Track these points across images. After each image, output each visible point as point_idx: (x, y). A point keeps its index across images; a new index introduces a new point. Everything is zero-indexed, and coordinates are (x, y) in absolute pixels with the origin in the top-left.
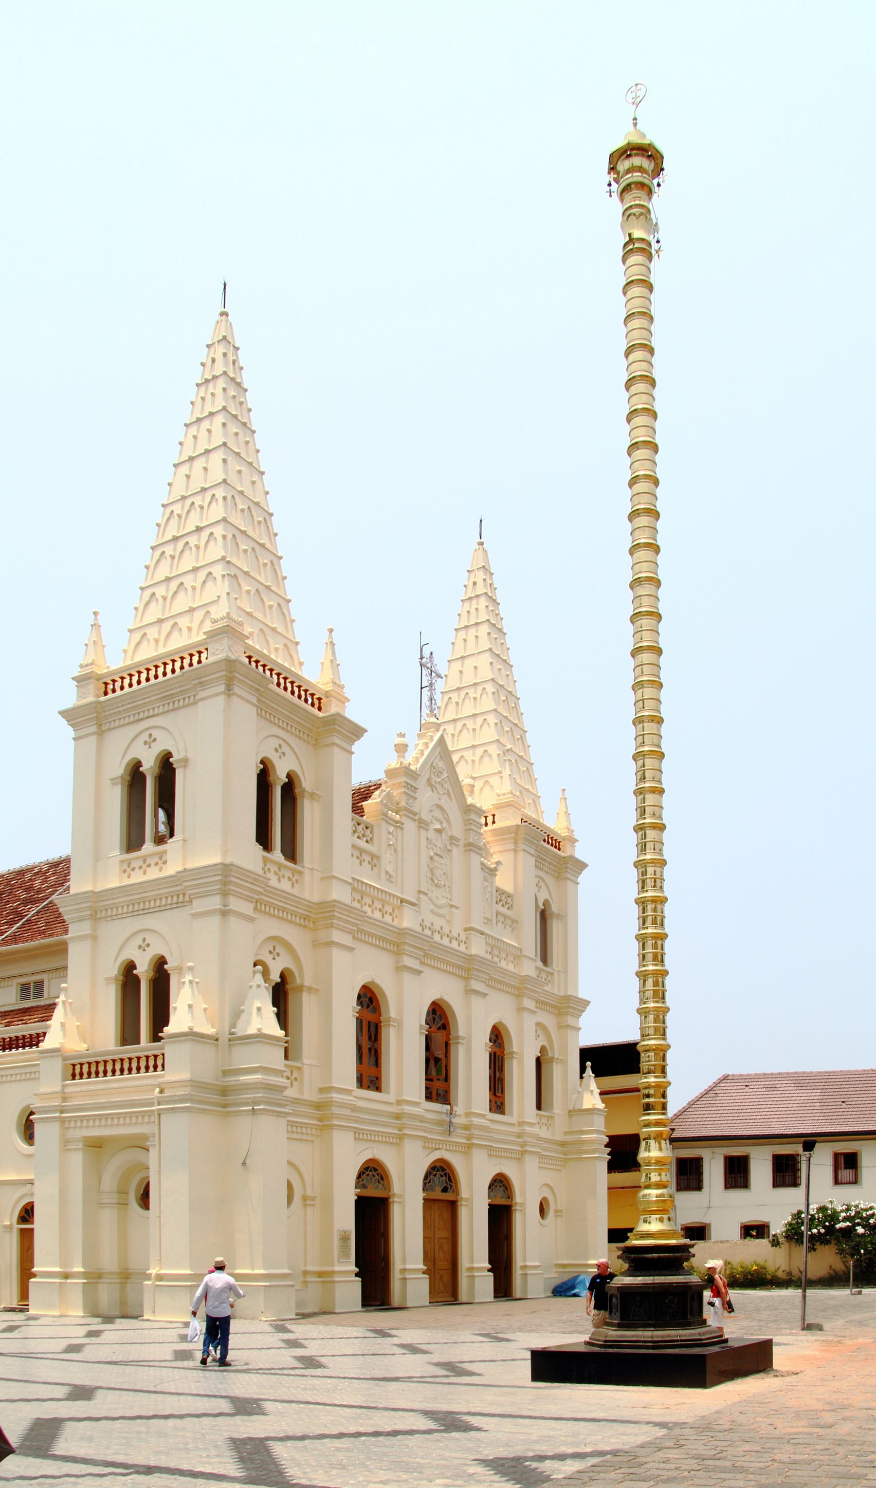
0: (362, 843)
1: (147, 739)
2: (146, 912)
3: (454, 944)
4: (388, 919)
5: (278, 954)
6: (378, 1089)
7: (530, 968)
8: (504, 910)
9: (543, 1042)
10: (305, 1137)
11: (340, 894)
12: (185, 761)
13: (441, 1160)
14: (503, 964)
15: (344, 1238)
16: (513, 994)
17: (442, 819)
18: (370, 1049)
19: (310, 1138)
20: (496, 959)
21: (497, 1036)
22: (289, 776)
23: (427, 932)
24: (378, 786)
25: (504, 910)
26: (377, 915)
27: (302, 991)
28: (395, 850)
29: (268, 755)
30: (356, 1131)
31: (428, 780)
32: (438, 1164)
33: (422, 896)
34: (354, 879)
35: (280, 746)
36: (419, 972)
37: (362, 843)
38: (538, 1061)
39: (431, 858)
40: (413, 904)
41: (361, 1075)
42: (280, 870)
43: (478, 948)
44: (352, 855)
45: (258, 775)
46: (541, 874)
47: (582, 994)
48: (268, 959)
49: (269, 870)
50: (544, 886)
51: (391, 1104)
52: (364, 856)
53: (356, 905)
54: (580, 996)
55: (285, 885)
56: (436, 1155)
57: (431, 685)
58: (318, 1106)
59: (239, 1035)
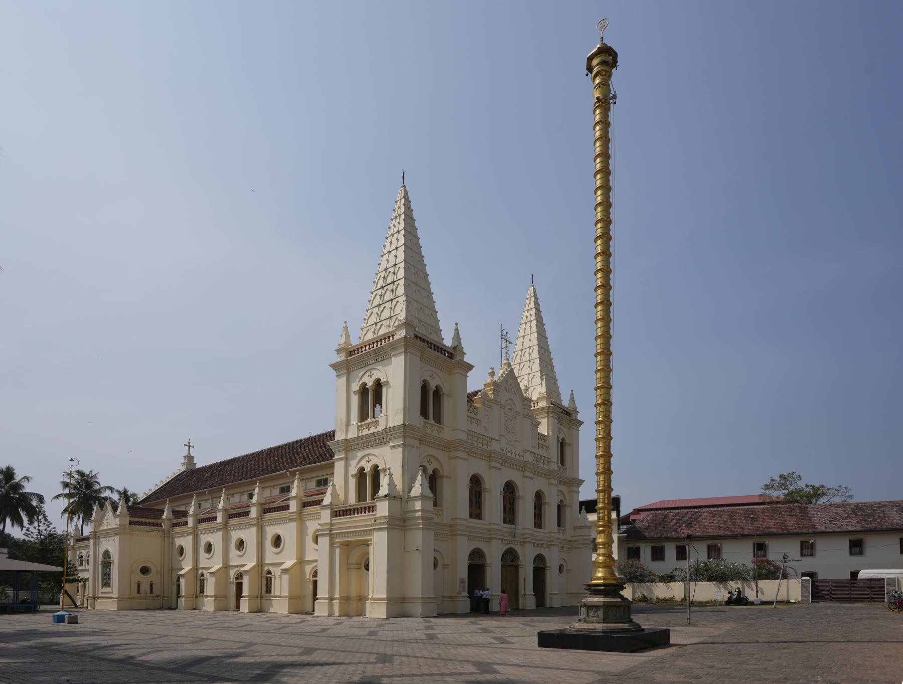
0: (472, 415)
1: (370, 374)
2: (370, 447)
3: (518, 457)
4: (485, 447)
5: (432, 462)
6: (480, 519)
7: (554, 466)
8: (542, 442)
9: (561, 497)
10: (444, 539)
11: (464, 437)
12: (387, 383)
13: (511, 548)
14: (542, 465)
15: (462, 581)
16: (547, 478)
17: (512, 404)
18: (476, 502)
19: (446, 539)
20: (538, 463)
21: (539, 496)
22: (436, 387)
23: (504, 452)
24: (481, 391)
25: (542, 442)
26: (480, 445)
27: (443, 478)
28: (489, 418)
29: (427, 379)
30: (468, 536)
31: (505, 388)
32: (509, 550)
33: (502, 437)
34: (468, 430)
35: (432, 374)
36: (500, 469)
37: (472, 415)
38: (559, 507)
39: (506, 421)
40: (498, 441)
41: (472, 513)
42: (432, 427)
43: (529, 458)
44: (468, 420)
45: (421, 387)
46: (561, 427)
47: (580, 477)
48: (427, 464)
49: (427, 427)
50: (562, 432)
51: (486, 525)
52: (473, 420)
53: (469, 441)
54: (580, 478)
55: (435, 433)
56: (509, 546)
57: (507, 347)
58: (451, 526)
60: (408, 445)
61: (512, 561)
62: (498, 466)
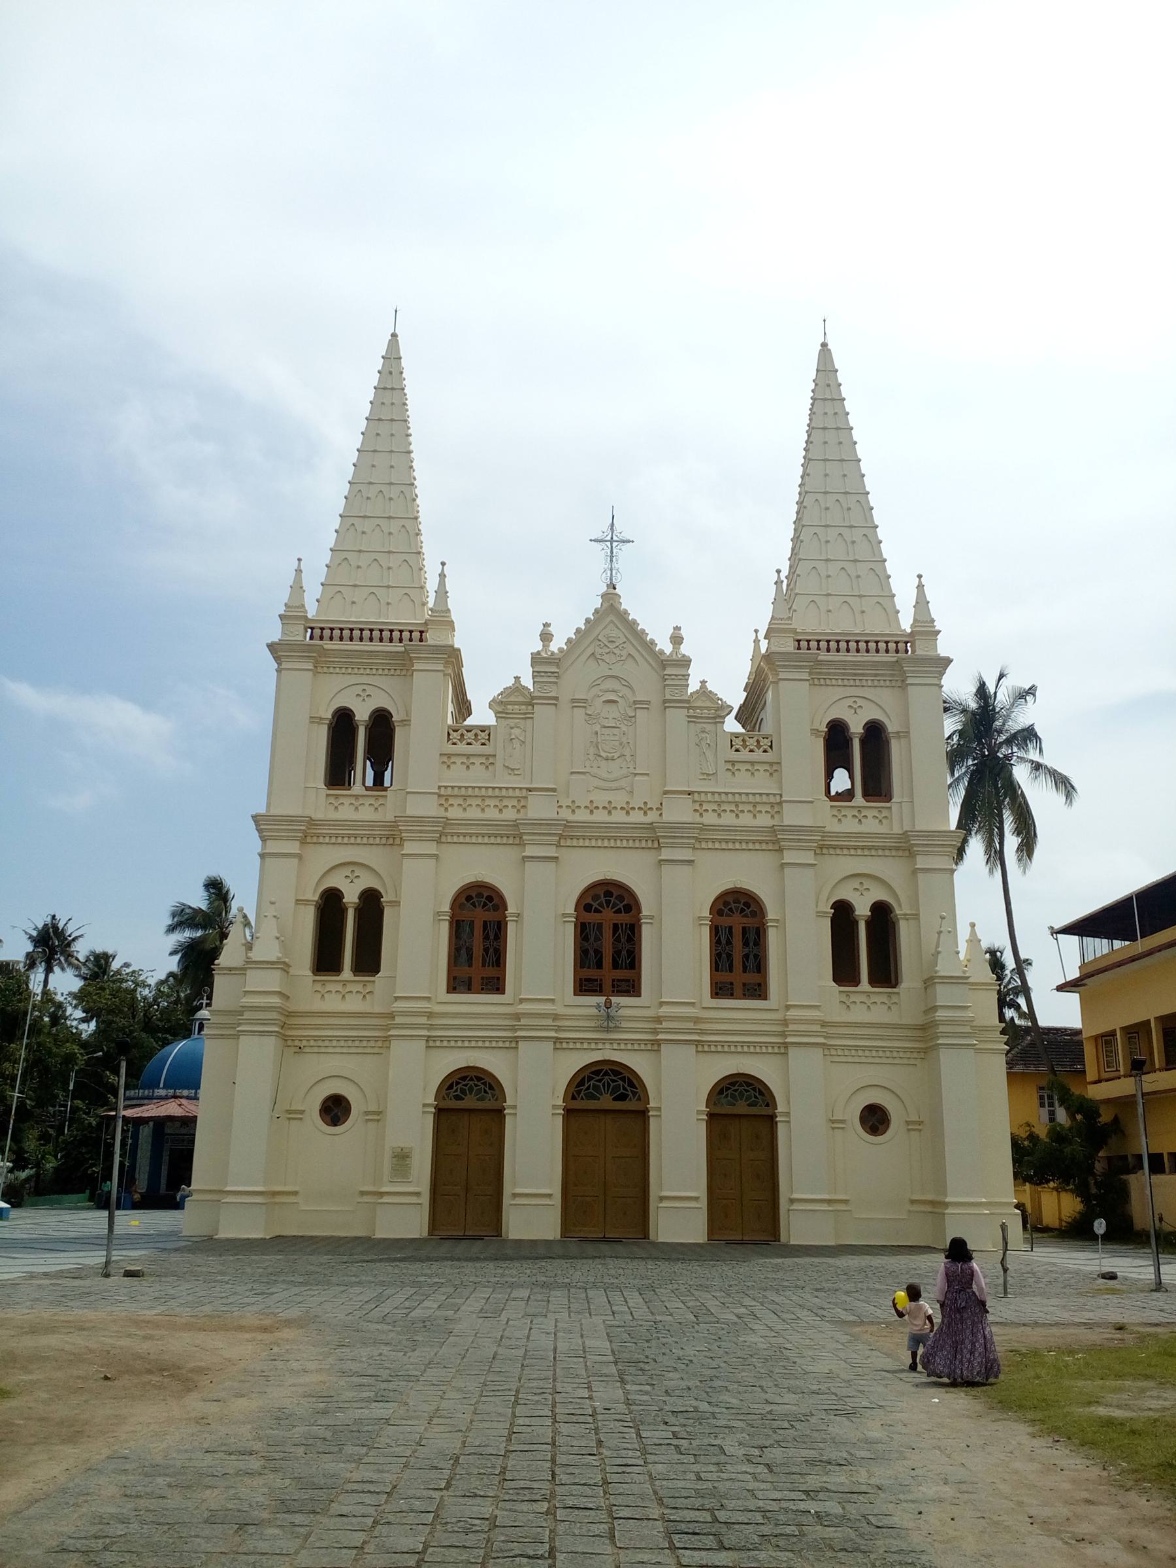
3: (637, 817)
8: (758, 755)
34: (439, 787)
43: (679, 812)
61: (622, 1098)
62: (551, 852)
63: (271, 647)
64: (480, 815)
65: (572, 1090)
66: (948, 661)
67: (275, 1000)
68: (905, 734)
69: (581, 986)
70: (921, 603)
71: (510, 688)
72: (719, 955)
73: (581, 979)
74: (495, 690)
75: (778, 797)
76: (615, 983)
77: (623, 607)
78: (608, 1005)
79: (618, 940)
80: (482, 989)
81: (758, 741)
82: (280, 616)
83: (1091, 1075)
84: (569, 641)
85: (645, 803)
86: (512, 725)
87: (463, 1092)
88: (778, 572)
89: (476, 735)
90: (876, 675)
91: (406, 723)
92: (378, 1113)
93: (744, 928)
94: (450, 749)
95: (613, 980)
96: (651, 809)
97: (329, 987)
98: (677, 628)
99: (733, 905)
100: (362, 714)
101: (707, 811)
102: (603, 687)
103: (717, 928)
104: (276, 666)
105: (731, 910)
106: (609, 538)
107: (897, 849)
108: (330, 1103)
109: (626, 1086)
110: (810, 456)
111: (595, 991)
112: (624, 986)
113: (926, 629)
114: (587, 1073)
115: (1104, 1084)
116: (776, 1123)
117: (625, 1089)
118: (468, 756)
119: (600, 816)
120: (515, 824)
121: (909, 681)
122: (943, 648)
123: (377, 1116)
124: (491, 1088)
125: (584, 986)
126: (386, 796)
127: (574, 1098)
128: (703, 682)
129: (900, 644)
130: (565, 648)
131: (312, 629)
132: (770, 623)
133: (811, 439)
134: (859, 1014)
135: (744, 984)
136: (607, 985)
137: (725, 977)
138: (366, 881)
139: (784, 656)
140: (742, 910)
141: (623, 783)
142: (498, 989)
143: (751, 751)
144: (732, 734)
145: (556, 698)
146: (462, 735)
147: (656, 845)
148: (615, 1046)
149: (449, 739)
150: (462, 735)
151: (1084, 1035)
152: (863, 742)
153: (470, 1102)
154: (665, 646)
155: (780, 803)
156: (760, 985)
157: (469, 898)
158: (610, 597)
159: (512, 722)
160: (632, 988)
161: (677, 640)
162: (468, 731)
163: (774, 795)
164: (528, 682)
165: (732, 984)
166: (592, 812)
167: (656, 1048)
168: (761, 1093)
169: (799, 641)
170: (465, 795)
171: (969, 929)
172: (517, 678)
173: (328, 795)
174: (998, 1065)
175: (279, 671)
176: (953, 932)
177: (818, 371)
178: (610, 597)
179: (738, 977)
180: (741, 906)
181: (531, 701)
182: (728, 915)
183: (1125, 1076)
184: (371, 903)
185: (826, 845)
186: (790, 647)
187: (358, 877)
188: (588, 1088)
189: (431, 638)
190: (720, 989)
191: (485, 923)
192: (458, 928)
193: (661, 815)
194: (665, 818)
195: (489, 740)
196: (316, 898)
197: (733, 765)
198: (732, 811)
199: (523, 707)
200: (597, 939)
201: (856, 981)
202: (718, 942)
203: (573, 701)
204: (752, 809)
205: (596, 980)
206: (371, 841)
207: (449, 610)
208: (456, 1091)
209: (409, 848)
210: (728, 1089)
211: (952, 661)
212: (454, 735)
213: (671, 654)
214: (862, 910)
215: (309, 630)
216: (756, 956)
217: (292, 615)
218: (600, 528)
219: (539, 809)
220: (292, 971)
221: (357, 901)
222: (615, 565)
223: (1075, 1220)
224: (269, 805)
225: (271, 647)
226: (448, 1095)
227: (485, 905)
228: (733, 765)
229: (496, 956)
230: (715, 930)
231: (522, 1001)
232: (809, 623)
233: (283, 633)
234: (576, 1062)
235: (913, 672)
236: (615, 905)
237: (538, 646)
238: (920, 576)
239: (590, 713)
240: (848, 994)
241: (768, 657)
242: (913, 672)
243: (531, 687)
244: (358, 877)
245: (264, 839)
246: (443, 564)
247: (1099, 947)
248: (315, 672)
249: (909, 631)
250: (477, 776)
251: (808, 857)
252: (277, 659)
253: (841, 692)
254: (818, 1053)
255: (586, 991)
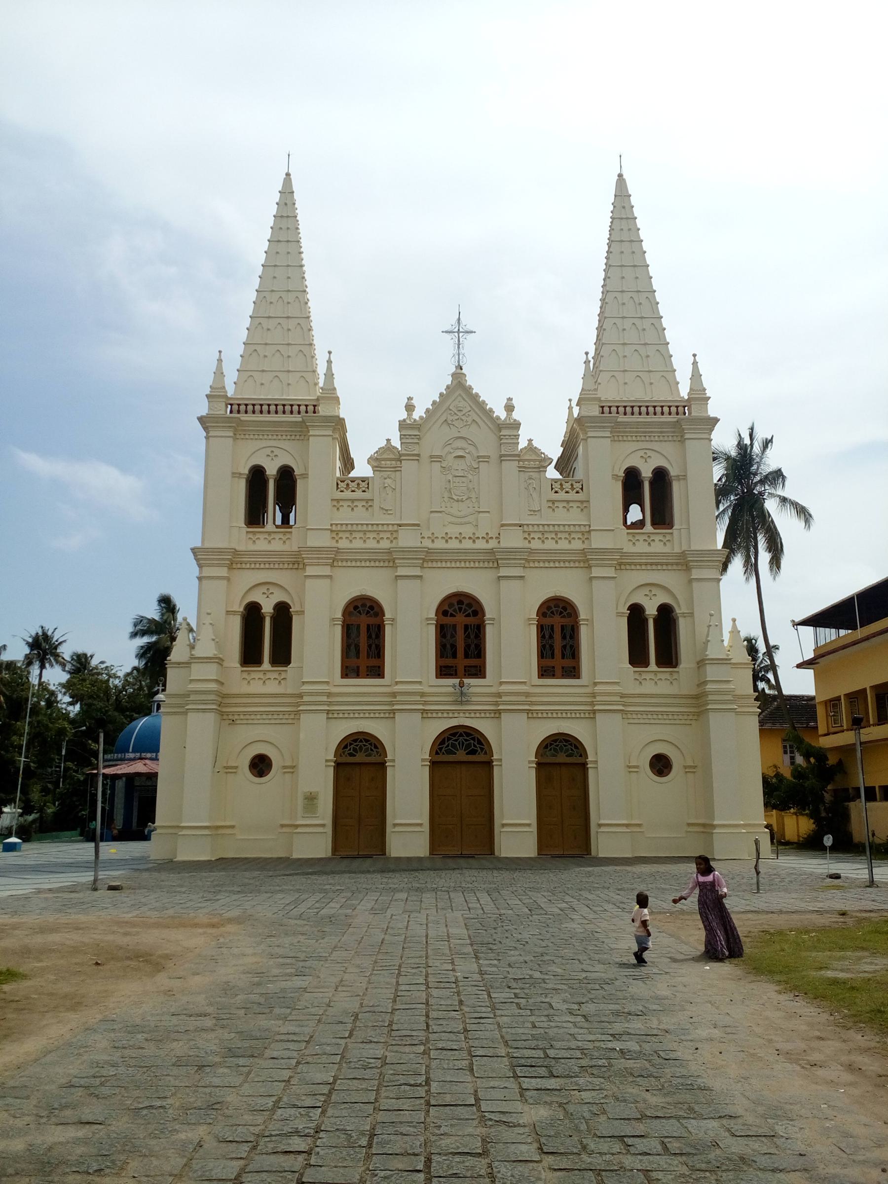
3: (481, 545)
8: (572, 496)
34: (331, 525)
43: (513, 540)
59: (197, 656)
60: (204, 577)
61: (473, 752)
62: (417, 572)
63: (201, 419)
64: (364, 546)
65: (436, 747)
66: (716, 420)
67: (213, 686)
68: (684, 477)
69: (441, 671)
70: (696, 376)
71: (383, 448)
72: (544, 646)
73: (441, 667)
74: (372, 450)
75: (587, 527)
76: (467, 668)
77: (468, 383)
78: (461, 685)
79: (468, 637)
80: (368, 675)
81: (572, 485)
82: (207, 396)
83: (822, 729)
84: (428, 410)
85: (487, 534)
86: (386, 477)
87: (355, 750)
88: (587, 353)
89: (358, 484)
90: (661, 432)
91: (305, 476)
92: (293, 767)
93: (562, 626)
94: (339, 496)
95: (465, 667)
96: (492, 538)
97: (253, 675)
98: (510, 399)
99: (554, 609)
100: (271, 470)
101: (533, 538)
102: (454, 446)
103: (542, 626)
104: (205, 434)
105: (552, 613)
106: (456, 330)
107: (677, 564)
108: (256, 761)
109: (476, 743)
110: (610, 263)
111: (452, 675)
112: (473, 670)
113: (699, 396)
114: (446, 735)
115: (831, 736)
116: (588, 768)
117: (475, 746)
118: (353, 501)
119: (454, 544)
120: (389, 552)
121: (687, 436)
122: (712, 410)
123: (291, 769)
124: (376, 747)
125: (443, 671)
126: (291, 532)
127: (437, 753)
128: (530, 441)
129: (679, 408)
130: (425, 416)
131: (231, 405)
132: (581, 394)
133: (611, 250)
134: (648, 688)
135: (563, 668)
136: (461, 670)
137: (549, 662)
138: (278, 597)
139: (592, 419)
140: (561, 613)
141: (471, 519)
142: (379, 675)
143: (567, 492)
144: (552, 480)
145: (418, 455)
146: (348, 485)
147: (496, 565)
148: (467, 715)
149: (338, 488)
150: (348, 485)
151: (817, 701)
152: (652, 483)
153: (360, 758)
154: (500, 413)
155: (589, 532)
156: (574, 668)
157: (356, 608)
158: (458, 376)
159: (385, 474)
160: (479, 672)
161: (509, 408)
162: (352, 482)
163: (585, 525)
164: (396, 443)
165: (553, 667)
166: (447, 541)
167: (497, 715)
168: (576, 747)
169: (603, 407)
170: (350, 530)
171: (731, 623)
172: (388, 440)
173: (247, 532)
174: (753, 723)
175: (207, 438)
176: (719, 626)
177: (615, 196)
178: (458, 376)
179: (558, 662)
180: (560, 609)
181: (399, 458)
182: (550, 617)
183: (847, 730)
184: (283, 613)
185: (623, 563)
186: (596, 411)
187: (272, 593)
188: (448, 746)
189: (322, 410)
190: (545, 671)
191: (368, 626)
192: (348, 630)
193: (499, 542)
194: (502, 545)
195: (368, 488)
196: (242, 609)
197: (553, 503)
198: (552, 538)
199: (394, 462)
200: (453, 636)
201: (646, 664)
202: (543, 637)
203: (431, 457)
204: (541, 536)
205: (452, 667)
206: (281, 566)
207: (335, 389)
208: (350, 749)
209: (310, 571)
210: (551, 744)
211: (719, 420)
212: (341, 485)
213: (505, 419)
214: (651, 610)
215: (229, 406)
216: (572, 647)
217: (215, 395)
218: (450, 322)
219: (407, 540)
220: (225, 664)
221: (272, 611)
222: (461, 351)
223: (809, 836)
224: (203, 542)
225: (201, 419)
226: (344, 753)
227: (368, 612)
228: (553, 503)
229: (377, 649)
230: (541, 628)
231: (397, 683)
232: (610, 393)
233: (210, 409)
234: (438, 727)
235: (690, 429)
236: (465, 611)
237: (404, 415)
238: (694, 355)
239: (444, 466)
240: (640, 673)
241: (579, 420)
242: (690, 429)
243: (399, 447)
244: (272, 593)
245: (200, 566)
246: (330, 353)
247: (829, 635)
248: (235, 438)
249: (686, 397)
250: (359, 516)
251: (610, 572)
252: (206, 429)
253: (634, 446)
254: (619, 716)
255: (445, 675)
